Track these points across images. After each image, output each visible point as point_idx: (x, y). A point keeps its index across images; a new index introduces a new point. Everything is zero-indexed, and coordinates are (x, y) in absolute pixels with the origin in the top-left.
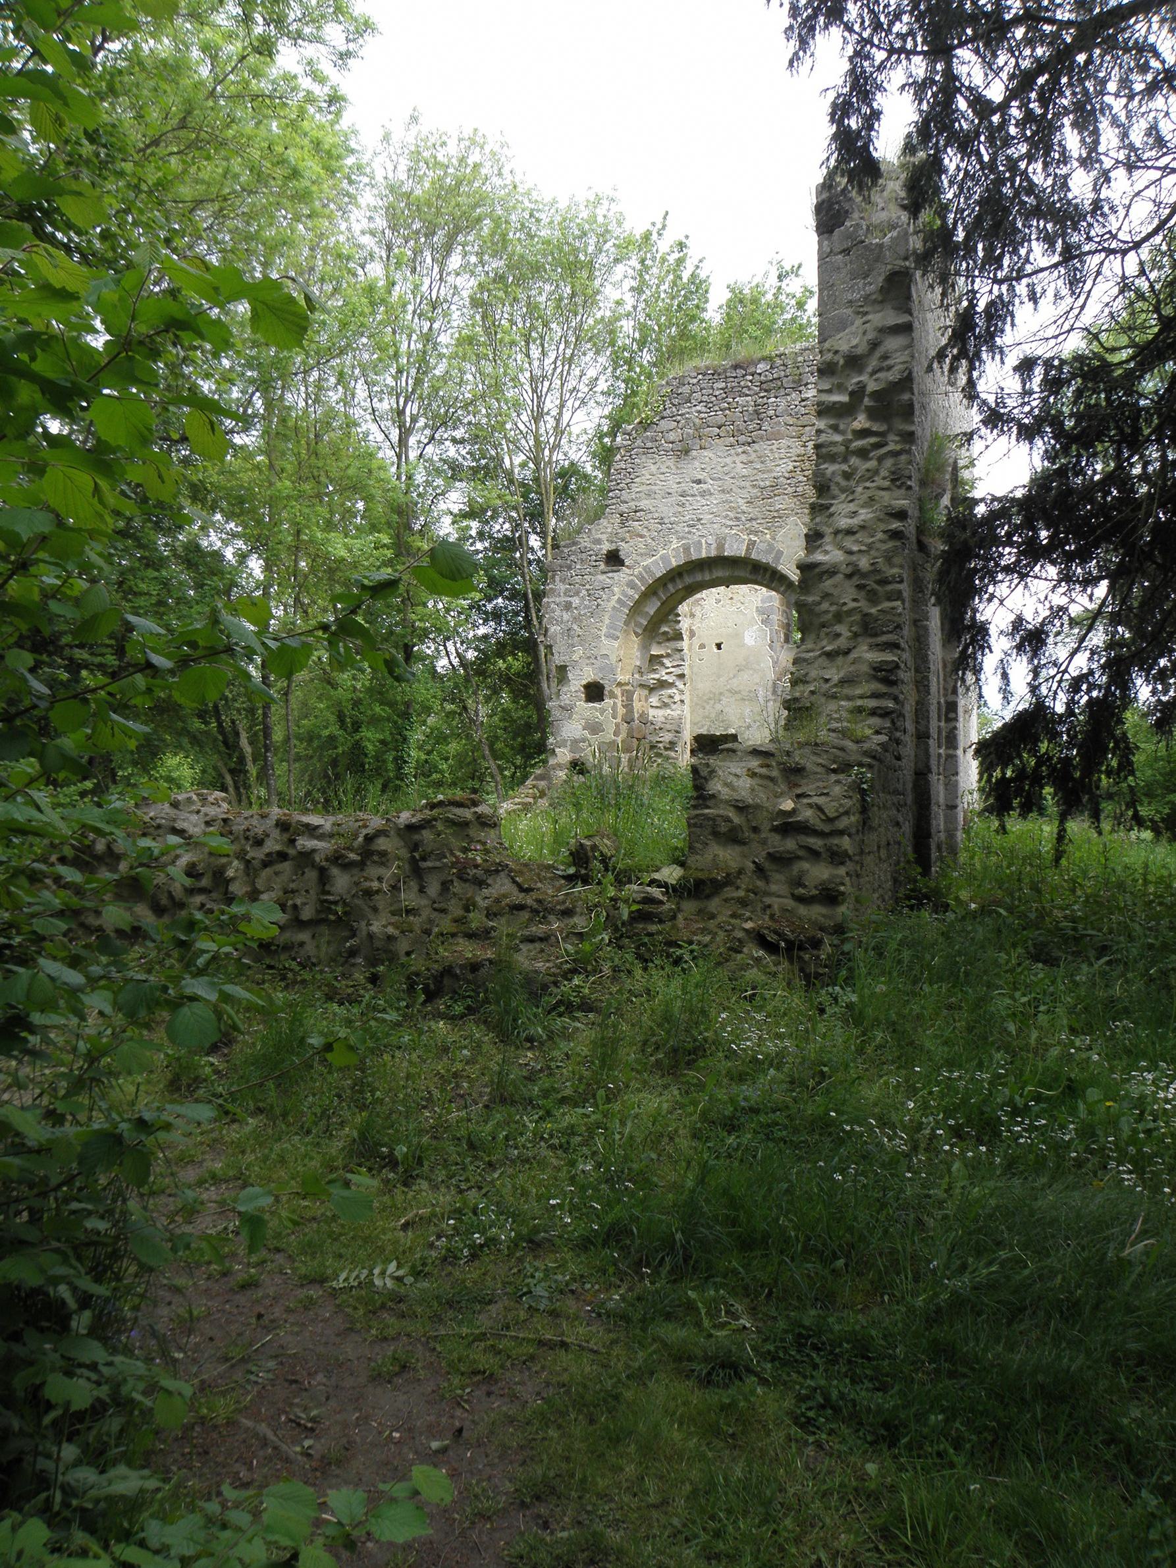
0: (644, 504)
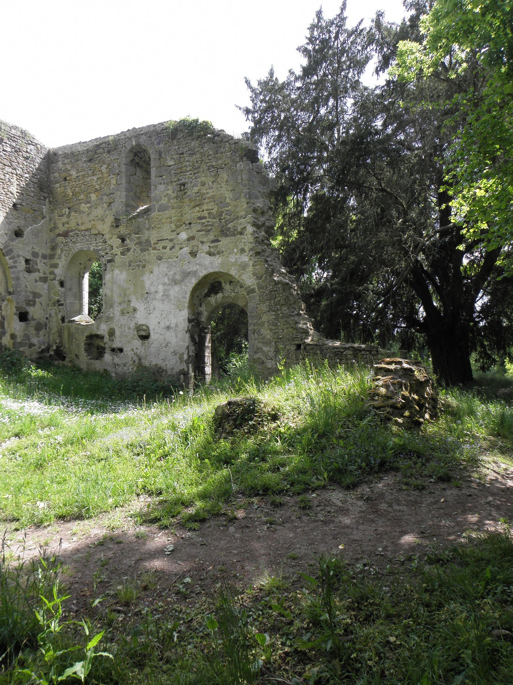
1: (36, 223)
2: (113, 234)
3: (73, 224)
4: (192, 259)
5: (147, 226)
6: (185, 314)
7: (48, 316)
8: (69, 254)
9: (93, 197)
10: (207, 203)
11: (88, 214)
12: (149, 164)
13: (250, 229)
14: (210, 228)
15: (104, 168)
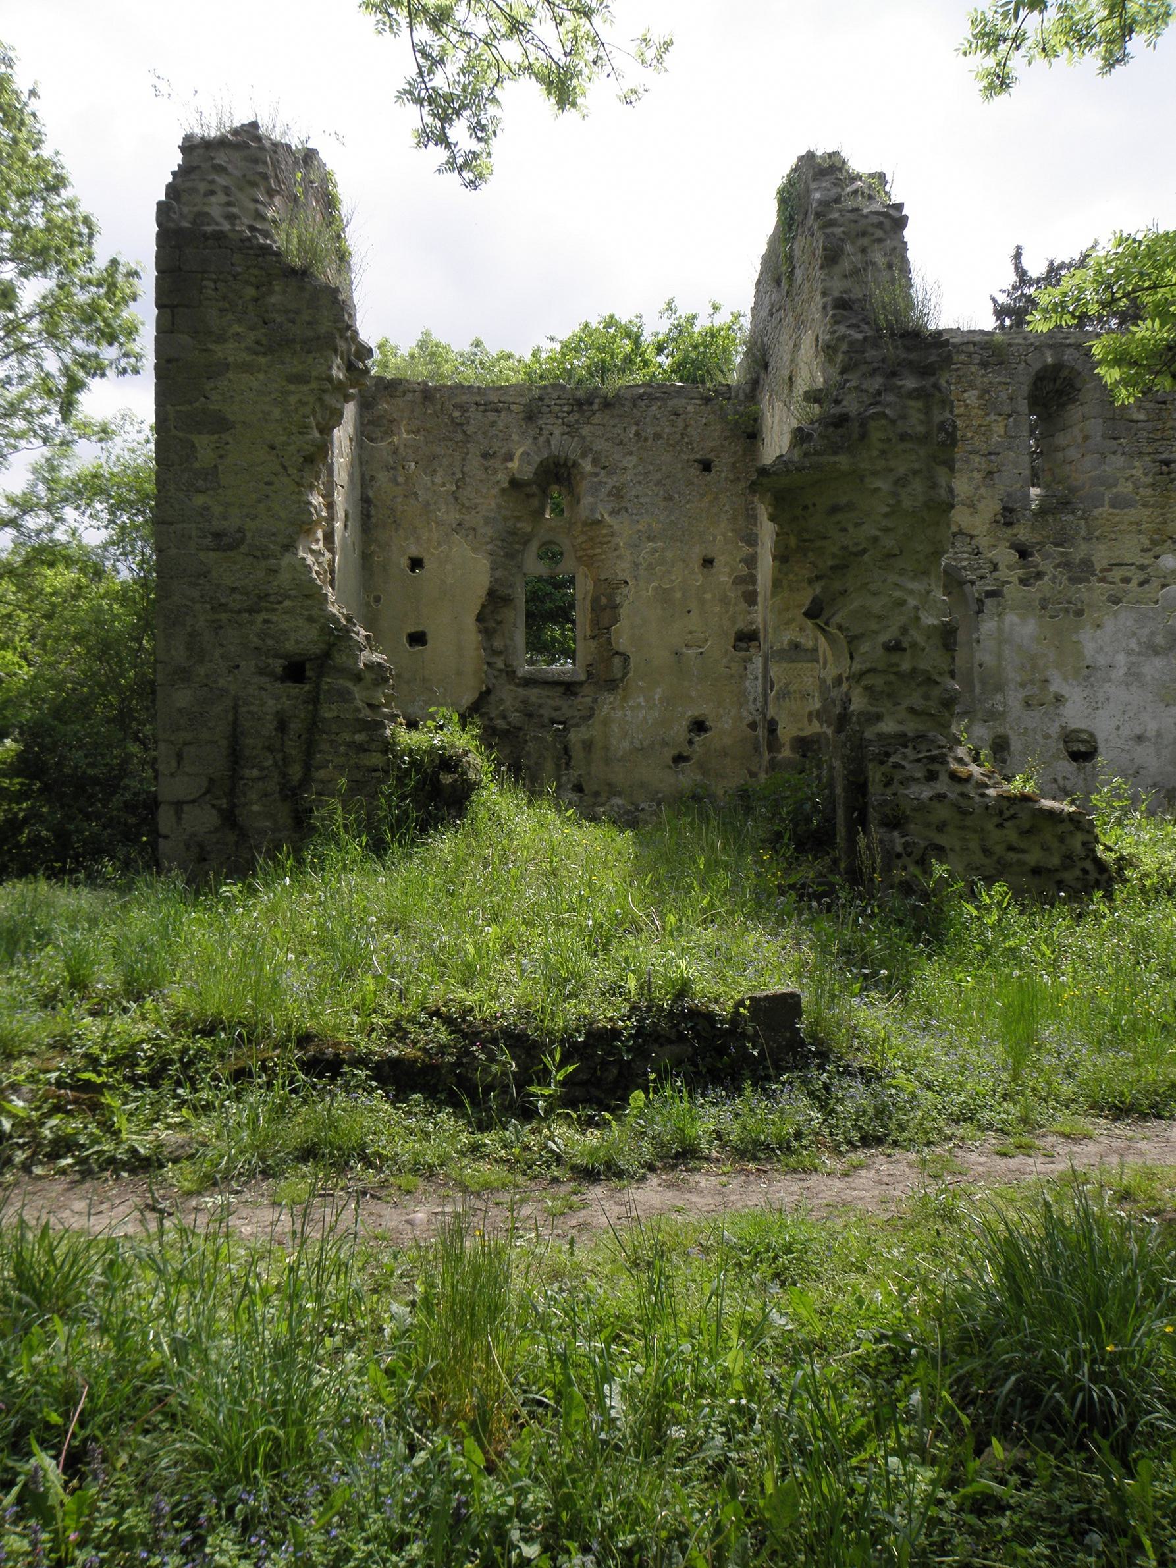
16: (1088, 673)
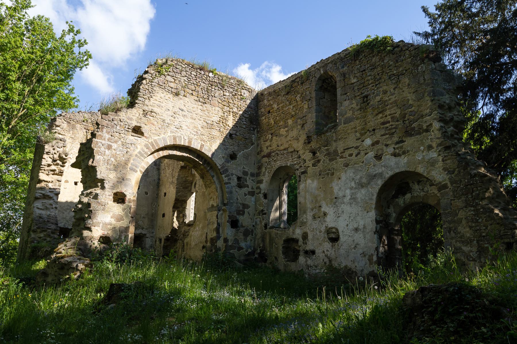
0: (156, 109)
1: (247, 148)
2: (305, 150)
3: (274, 146)
4: (378, 163)
5: (334, 138)
6: (372, 214)
7: (254, 224)
8: (271, 171)
9: (290, 122)
10: (389, 109)
11: (286, 136)
12: (335, 88)
13: (436, 125)
14: (394, 130)
15: (298, 98)
16: (335, 201)
